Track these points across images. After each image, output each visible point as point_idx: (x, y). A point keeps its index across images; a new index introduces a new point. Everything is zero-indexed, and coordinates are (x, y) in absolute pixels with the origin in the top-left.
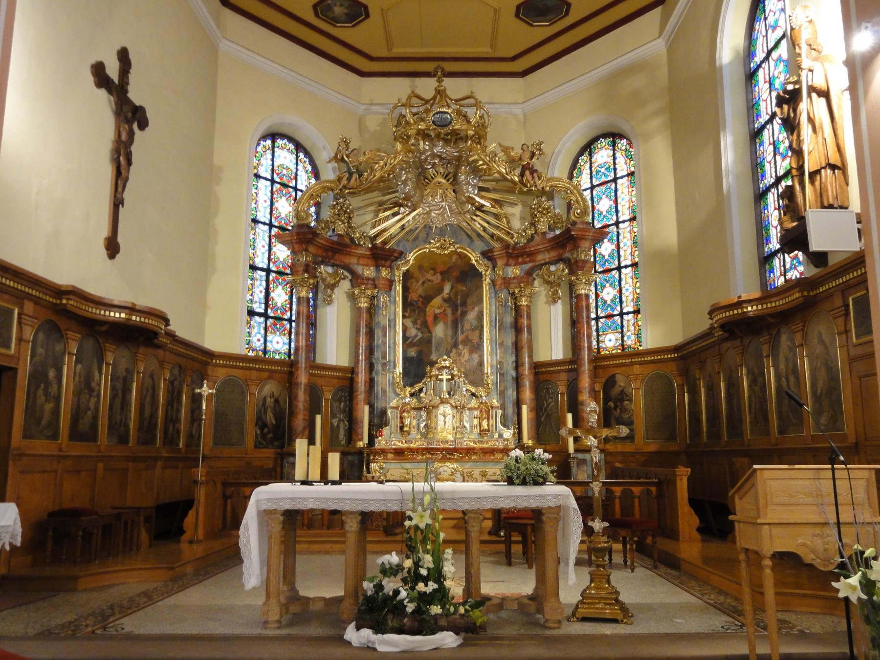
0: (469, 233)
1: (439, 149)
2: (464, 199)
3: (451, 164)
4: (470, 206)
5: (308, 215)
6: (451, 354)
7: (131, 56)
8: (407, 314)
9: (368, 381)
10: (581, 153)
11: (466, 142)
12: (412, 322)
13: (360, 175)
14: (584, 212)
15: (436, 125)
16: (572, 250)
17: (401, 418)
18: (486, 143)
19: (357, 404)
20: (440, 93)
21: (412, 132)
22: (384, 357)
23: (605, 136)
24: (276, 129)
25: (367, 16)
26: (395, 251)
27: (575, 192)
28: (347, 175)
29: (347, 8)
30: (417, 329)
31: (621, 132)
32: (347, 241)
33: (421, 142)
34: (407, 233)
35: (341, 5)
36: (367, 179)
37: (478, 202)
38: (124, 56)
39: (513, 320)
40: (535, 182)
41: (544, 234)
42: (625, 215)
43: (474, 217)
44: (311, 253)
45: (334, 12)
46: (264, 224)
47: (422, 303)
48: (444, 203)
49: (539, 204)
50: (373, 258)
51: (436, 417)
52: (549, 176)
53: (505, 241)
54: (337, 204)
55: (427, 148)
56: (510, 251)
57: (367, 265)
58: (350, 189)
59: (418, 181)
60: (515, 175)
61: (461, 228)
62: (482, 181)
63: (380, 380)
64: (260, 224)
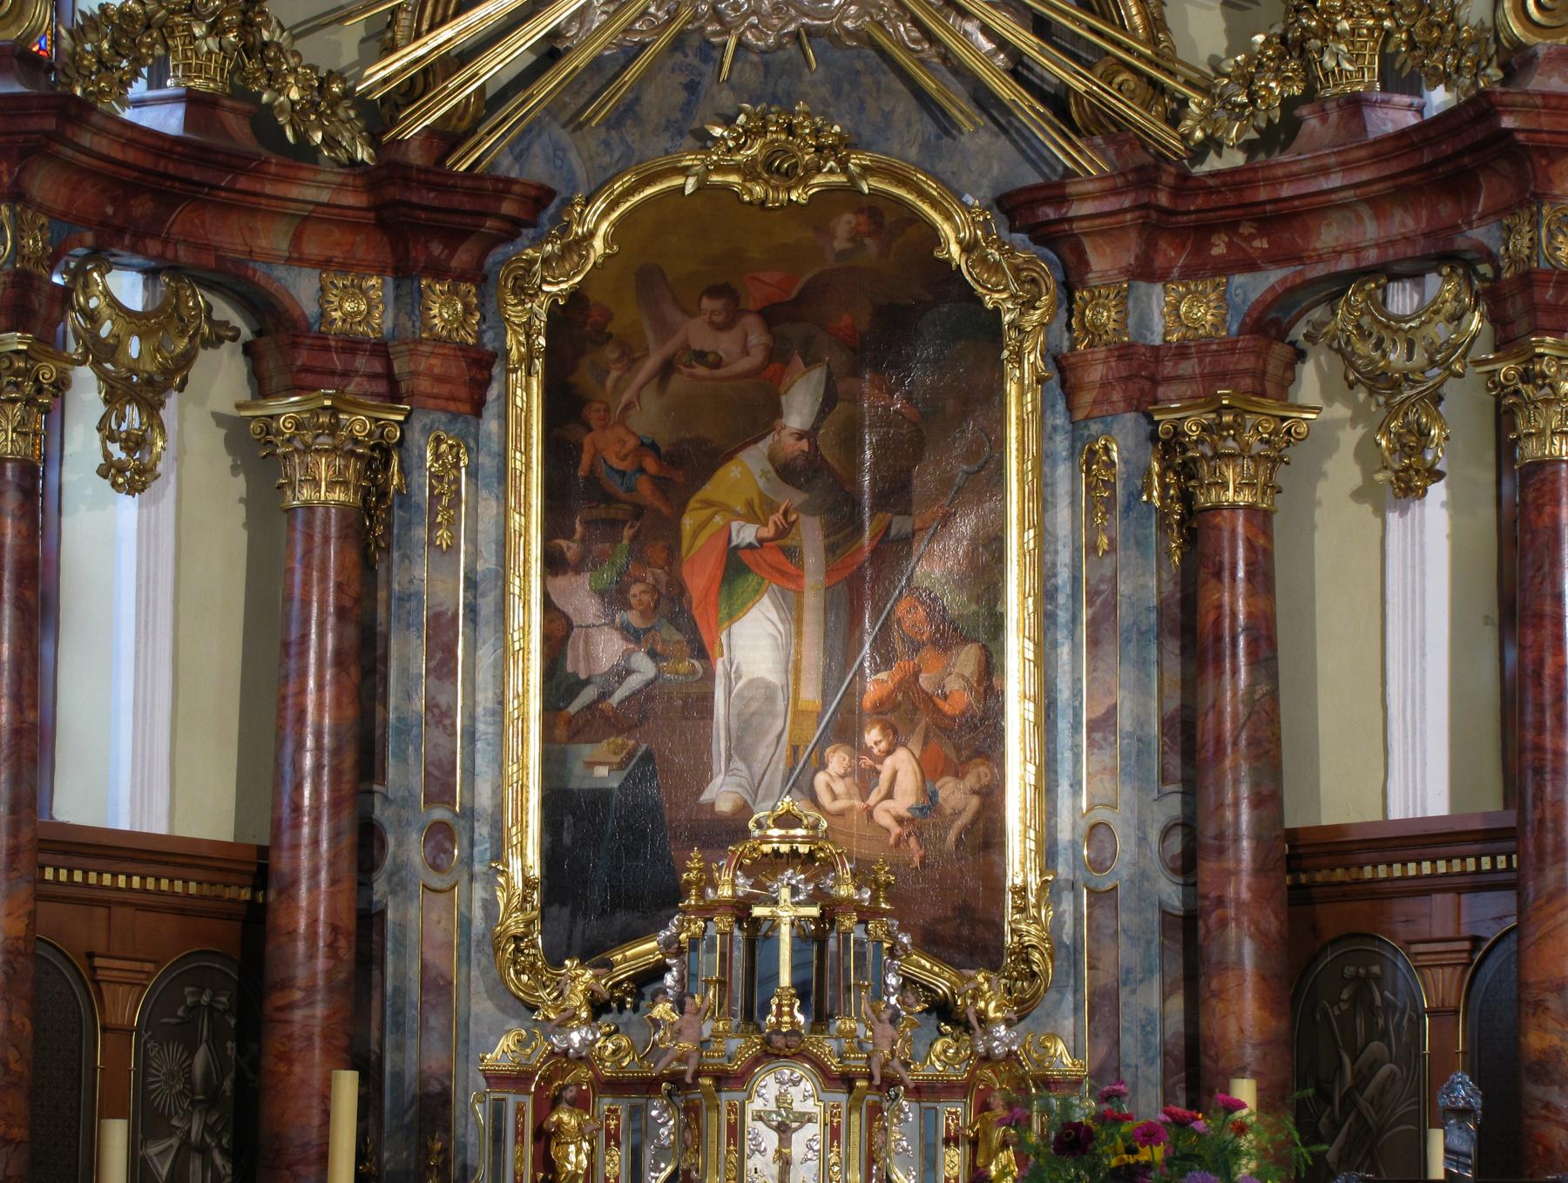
0: (930, 84)
6: (821, 779)
8: (571, 549)
9: (348, 921)
12: (601, 594)
16: (1508, 210)
17: (545, 1137)
19: (286, 1058)
22: (440, 788)
26: (504, 186)
30: (631, 634)
32: (238, 129)
34: (575, 83)
39: (1169, 588)
41: (1355, 105)
44: (41, 209)
47: (661, 484)
50: (382, 225)
51: (736, 1132)
53: (1141, 140)
56: (1163, 199)
57: (344, 269)
63: (413, 912)
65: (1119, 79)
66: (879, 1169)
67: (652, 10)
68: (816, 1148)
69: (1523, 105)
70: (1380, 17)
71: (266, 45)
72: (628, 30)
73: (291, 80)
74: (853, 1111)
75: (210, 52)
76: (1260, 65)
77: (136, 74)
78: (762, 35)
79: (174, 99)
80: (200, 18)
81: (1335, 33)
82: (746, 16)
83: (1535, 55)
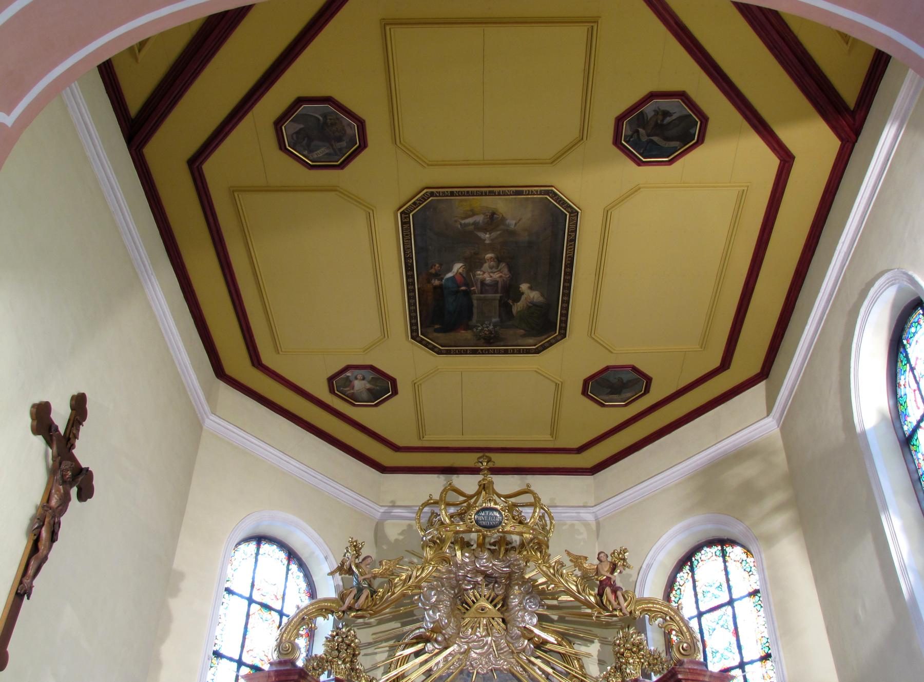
1: (485, 562)
2: (519, 633)
3: (500, 583)
4: (526, 642)
5: (294, 648)
7: (89, 406)
10: (679, 567)
11: (520, 553)
13: (373, 592)
14: (693, 646)
15: (480, 526)
18: (550, 551)
20: (484, 487)
21: (448, 535)
23: (710, 543)
24: (264, 529)
25: (395, 392)
27: (678, 618)
28: (355, 591)
29: (369, 382)
31: (733, 538)
33: (459, 553)
35: (364, 379)
36: (382, 598)
37: (539, 636)
38: (79, 405)
40: (619, 604)
42: (752, 651)
43: (533, 659)
45: (353, 388)
46: (231, 659)
48: (490, 639)
49: (626, 638)
52: (637, 595)
54: (337, 634)
55: (467, 560)
58: (358, 610)
59: (454, 604)
60: (590, 594)
61: (513, 674)
62: (543, 606)
64: (224, 660)
65: (574, 680)
67: (455, 663)
69: (684, 672)
70: (640, 659)
71: (357, 669)
72: (449, 668)
73: (363, 679)
75: (342, 669)
76: (610, 674)
77: (323, 673)
78: (483, 670)
79: (332, 680)
80: (340, 659)
81: (629, 663)
82: (479, 665)
83: (684, 662)
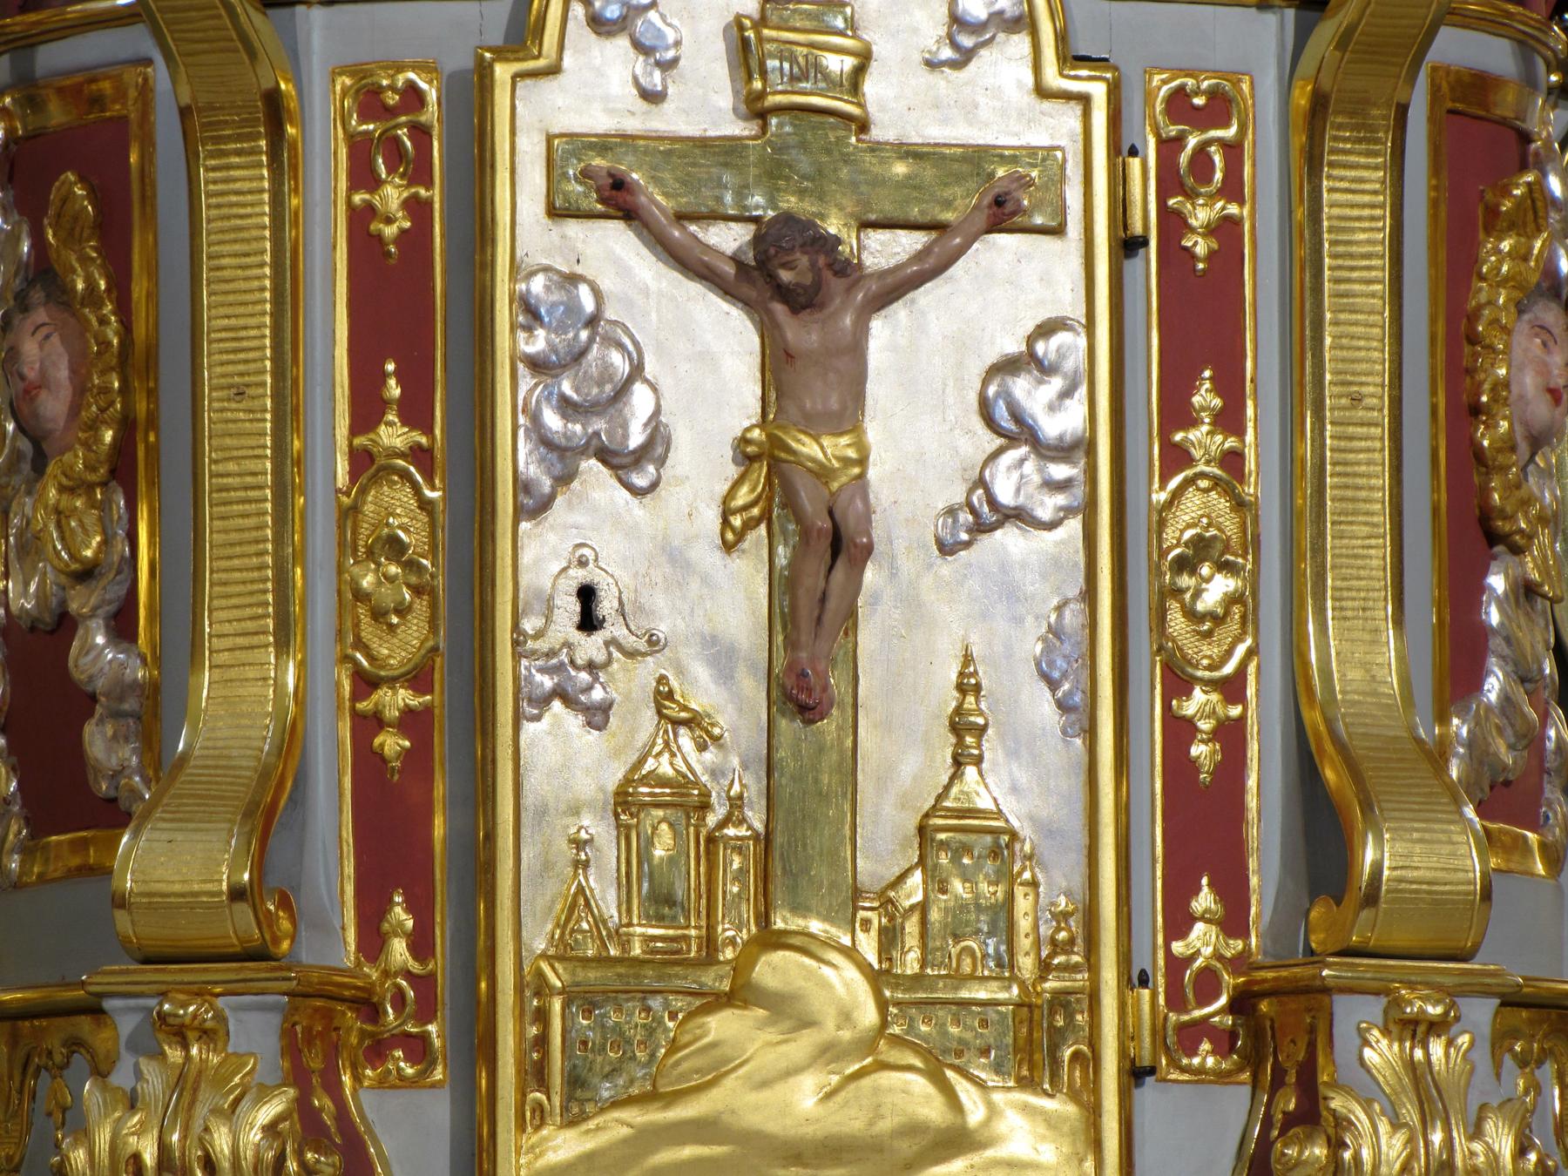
66: (1526, 592)
68: (1064, 422)
74: (1338, 139)
